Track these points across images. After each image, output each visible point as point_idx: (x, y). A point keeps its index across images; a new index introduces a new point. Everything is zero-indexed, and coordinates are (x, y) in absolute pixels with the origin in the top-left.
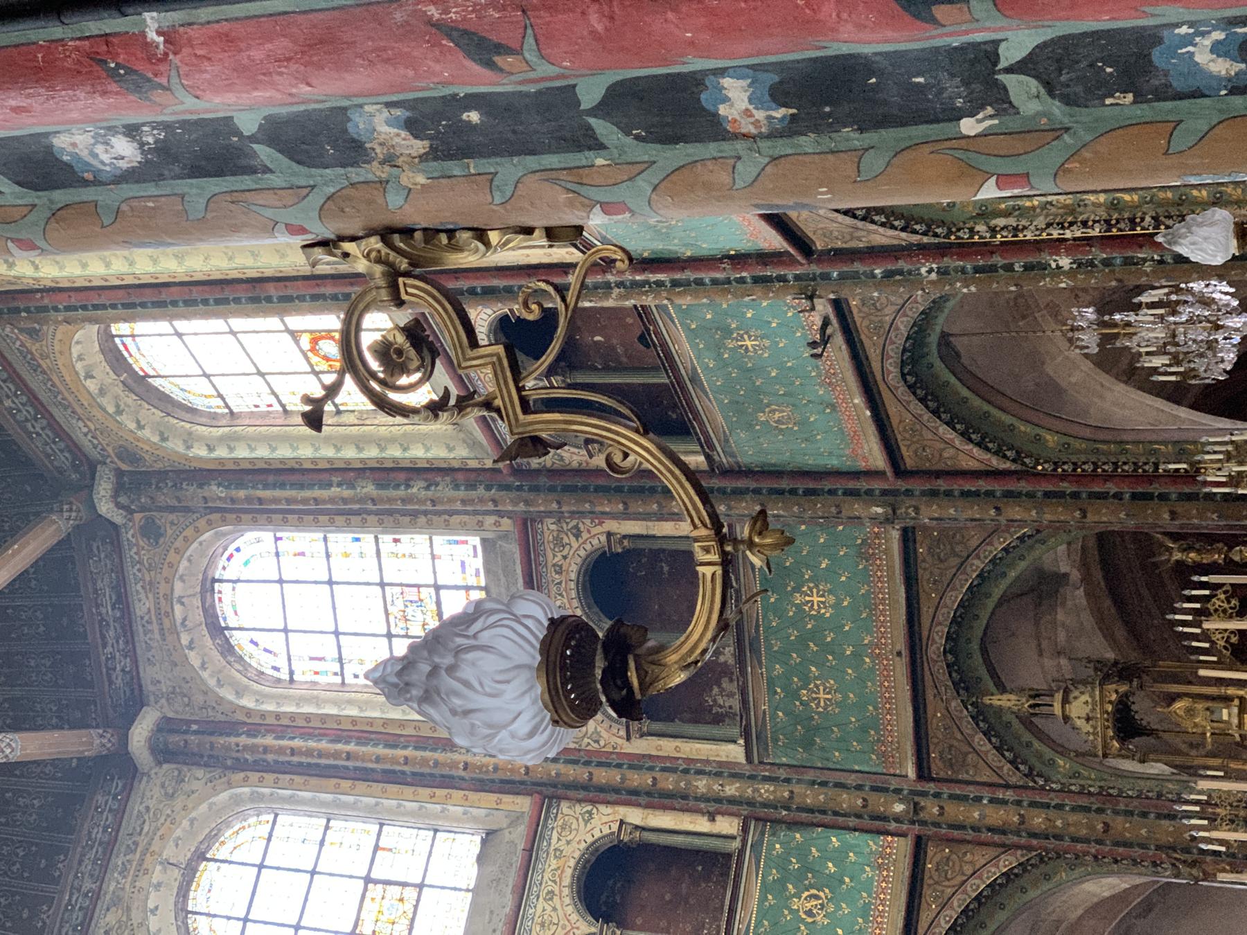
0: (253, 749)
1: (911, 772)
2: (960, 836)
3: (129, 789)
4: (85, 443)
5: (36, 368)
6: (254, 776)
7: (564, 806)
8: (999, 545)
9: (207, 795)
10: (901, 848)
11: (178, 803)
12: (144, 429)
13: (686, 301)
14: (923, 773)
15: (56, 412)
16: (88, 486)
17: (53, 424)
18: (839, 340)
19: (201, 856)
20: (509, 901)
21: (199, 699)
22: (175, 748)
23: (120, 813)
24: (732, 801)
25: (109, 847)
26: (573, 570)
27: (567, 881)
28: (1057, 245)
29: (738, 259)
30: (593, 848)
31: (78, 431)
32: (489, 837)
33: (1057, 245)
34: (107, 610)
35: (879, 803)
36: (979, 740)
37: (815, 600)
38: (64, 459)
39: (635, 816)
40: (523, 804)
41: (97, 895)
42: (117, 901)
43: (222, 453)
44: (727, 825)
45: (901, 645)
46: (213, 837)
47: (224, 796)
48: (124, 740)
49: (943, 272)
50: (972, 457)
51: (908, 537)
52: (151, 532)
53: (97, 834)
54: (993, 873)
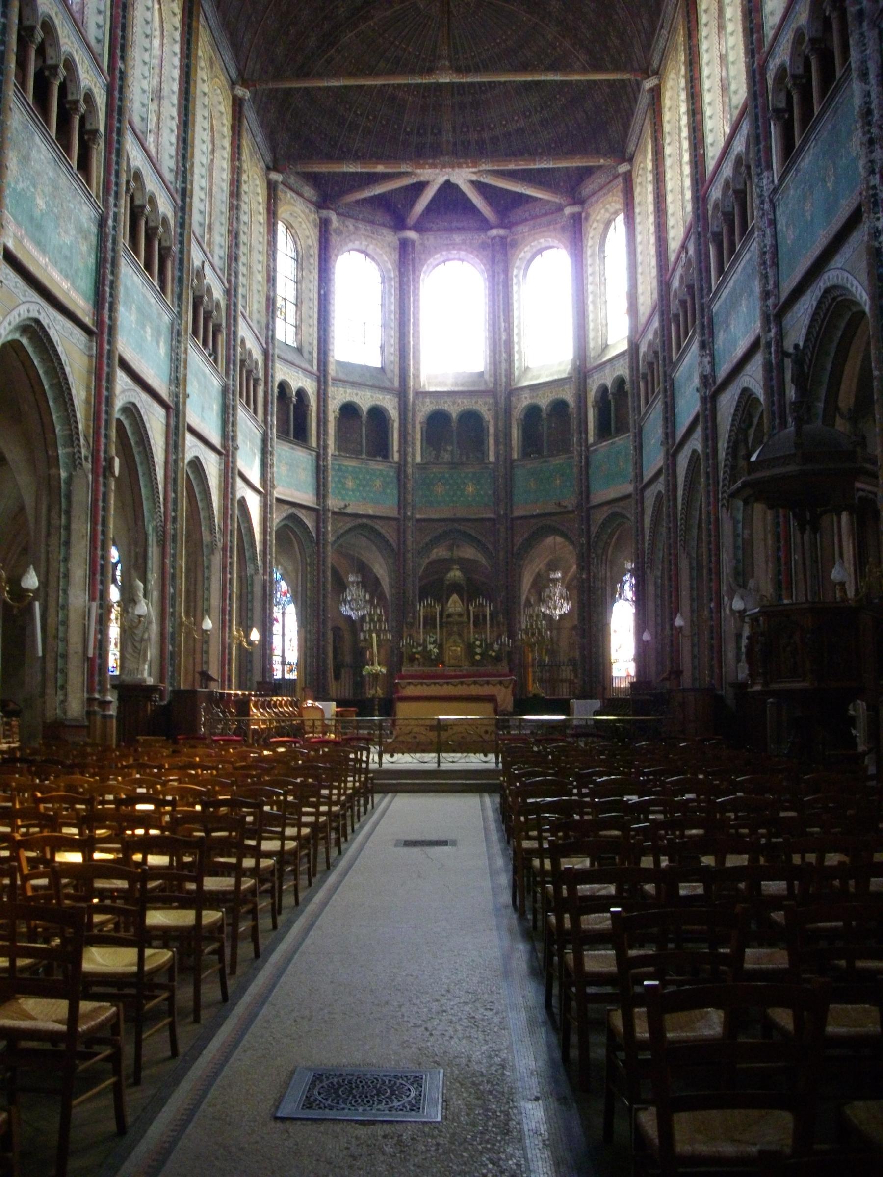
0: (408, 281)
1: (418, 516)
2: (401, 532)
3: (390, 227)
4: (520, 228)
5: (549, 224)
6: (397, 279)
7: (397, 400)
8: (490, 547)
9: (390, 260)
10: (394, 514)
11: (387, 249)
12: (524, 253)
13: (575, 470)
14: (418, 521)
15: (531, 223)
16: (501, 226)
17: (526, 220)
18: (559, 510)
19: (367, 255)
20: (370, 383)
21: (423, 257)
22: (404, 247)
23: (383, 225)
24: (405, 461)
25: (372, 222)
26: (476, 407)
27: (378, 403)
28: (589, 573)
29: (588, 487)
30: (386, 410)
31: (523, 228)
32: (383, 369)
33: (589, 573)
34: (455, 224)
35: (409, 508)
36: (428, 538)
37: (470, 489)
38: (511, 219)
39: (396, 425)
40: (396, 384)
41: (357, 219)
42: (356, 228)
43: (515, 281)
44: (396, 457)
45: (459, 515)
46: (373, 259)
47: (390, 266)
48: (410, 229)
49: (582, 545)
50: (519, 541)
51: (494, 520)
52: (483, 246)
53: (377, 218)
54: (391, 540)
